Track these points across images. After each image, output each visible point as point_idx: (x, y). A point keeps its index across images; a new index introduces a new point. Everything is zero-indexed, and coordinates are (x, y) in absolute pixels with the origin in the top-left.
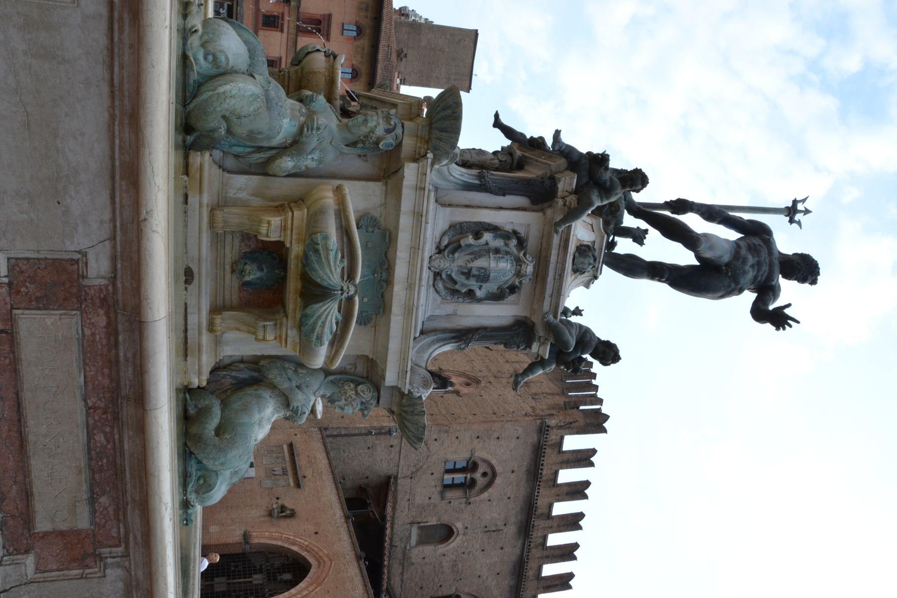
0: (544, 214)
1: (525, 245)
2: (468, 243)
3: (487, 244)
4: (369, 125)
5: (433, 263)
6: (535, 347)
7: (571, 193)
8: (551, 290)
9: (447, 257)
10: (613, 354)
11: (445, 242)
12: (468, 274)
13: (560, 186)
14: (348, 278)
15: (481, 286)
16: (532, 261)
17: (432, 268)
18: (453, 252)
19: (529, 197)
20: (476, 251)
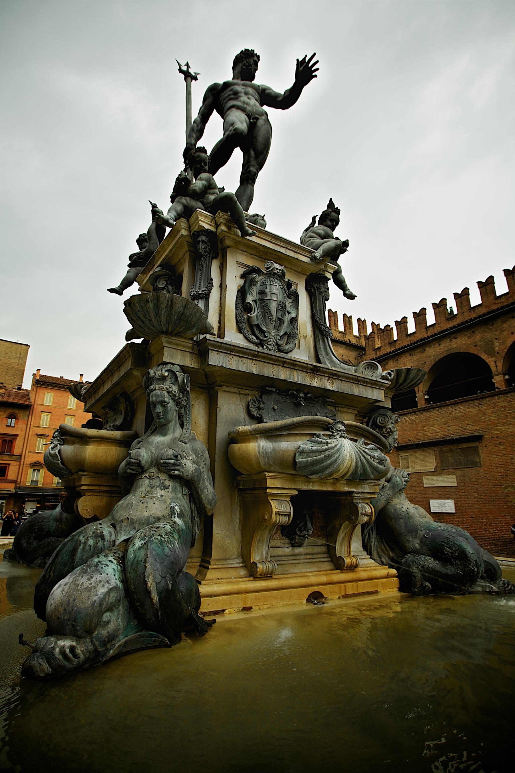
2: (256, 317)
3: (255, 301)
4: (166, 399)
6: (329, 276)
8: (291, 251)
9: (267, 339)
12: (281, 321)
14: (327, 429)
18: (263, 332)
20: (261, 312)
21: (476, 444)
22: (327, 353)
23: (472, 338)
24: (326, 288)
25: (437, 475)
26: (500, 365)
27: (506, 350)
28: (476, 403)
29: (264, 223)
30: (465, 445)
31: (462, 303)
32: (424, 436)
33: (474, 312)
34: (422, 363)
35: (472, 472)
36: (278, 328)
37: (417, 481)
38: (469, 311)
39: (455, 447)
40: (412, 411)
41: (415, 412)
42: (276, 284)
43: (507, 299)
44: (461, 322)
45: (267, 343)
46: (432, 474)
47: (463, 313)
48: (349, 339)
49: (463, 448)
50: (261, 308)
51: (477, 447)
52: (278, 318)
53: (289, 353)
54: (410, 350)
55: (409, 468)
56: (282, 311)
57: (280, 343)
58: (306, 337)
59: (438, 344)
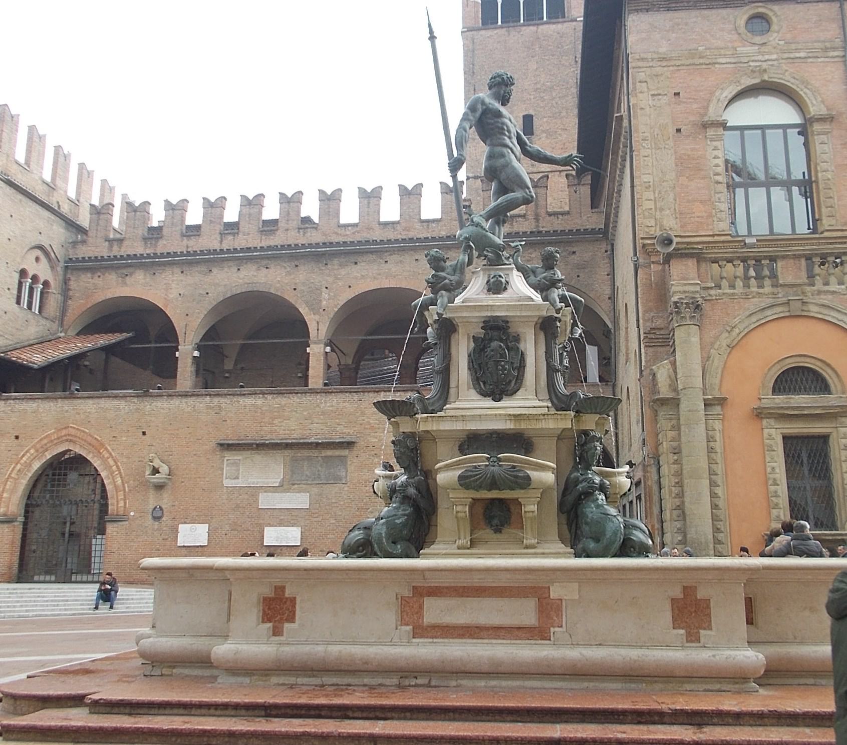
21: (345, 452)
23: (292, 276)
25: (282, 492)
26: (324, 329)
27: (336, 310)
28: (356, 397)
30: (329, 453)
31: (288, 214)
32: (271, 432)
33: (304, 235)
34: (201, 292)
35: (332, 490)
37: (248, 499)
38: (297, 230)
39: (314, 453)
40: (258, 392)
41: (263, 394)
43: (354, 233)
44: (282, 244)
46: (275, 489)
47: (287, 230)
48: (58, 203)
49: (326, 457)
51: (345, 457)
54: (183, 263)
55: (238, 478)
59: (236, 270)
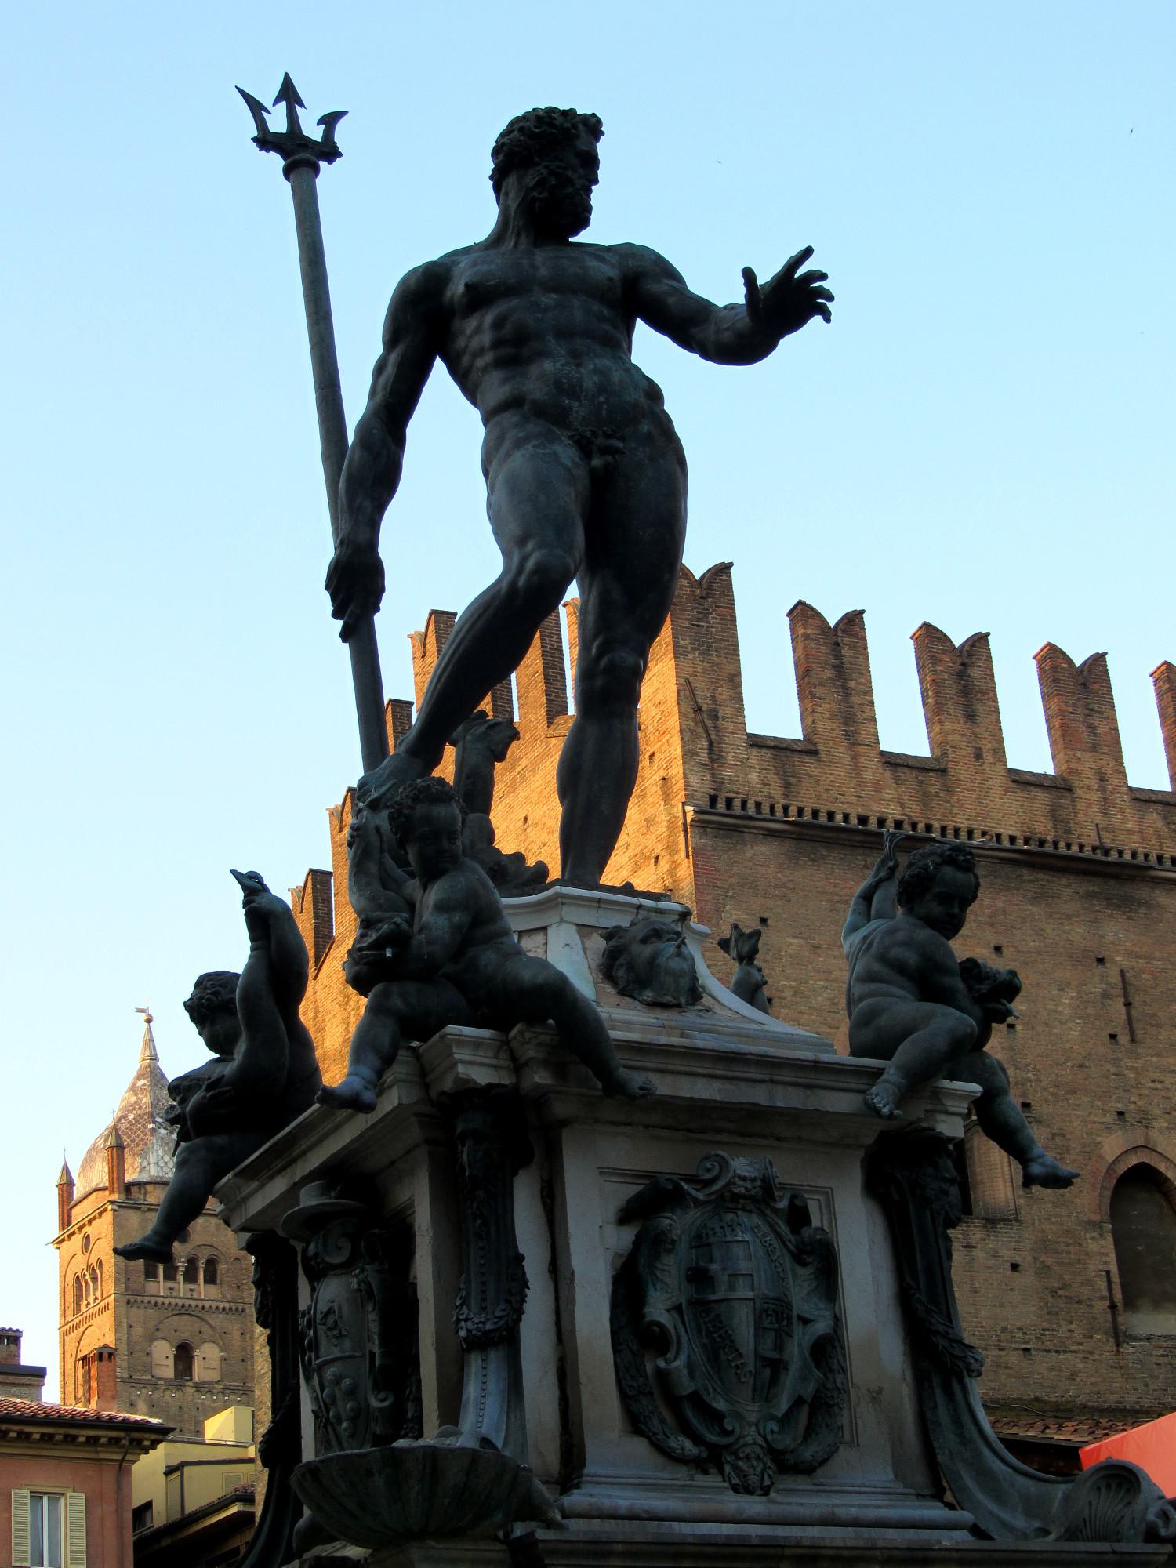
0: (564, 1123)
1: (670, 1187)
2: (685, 1371)
3: (678, 1308)
5: (753, 1479)
6: (951, 1127)
7: (508, 1042)
8: (790, 1089)
10: (948, 871)
11: (685, 1445)
12: (776, 1366)
13: (482, 1076)
15: (800, 1318)
16: (724, 1164)
17: (767, 1482)
18: (715, 1418)
19: (515, 1173)
20: (704, 1346)
22: (964, 1439)
24: (945, 1180)
29: (685, 966)
36: (765, 1392)
42: (747, 1237)
45: (735, 1453)
50: (700, 1332)
52: (764, 1359)
53: (819, 1471)
56: (776, 1330)
57: (785, 1441)
58: (880, 1391)
